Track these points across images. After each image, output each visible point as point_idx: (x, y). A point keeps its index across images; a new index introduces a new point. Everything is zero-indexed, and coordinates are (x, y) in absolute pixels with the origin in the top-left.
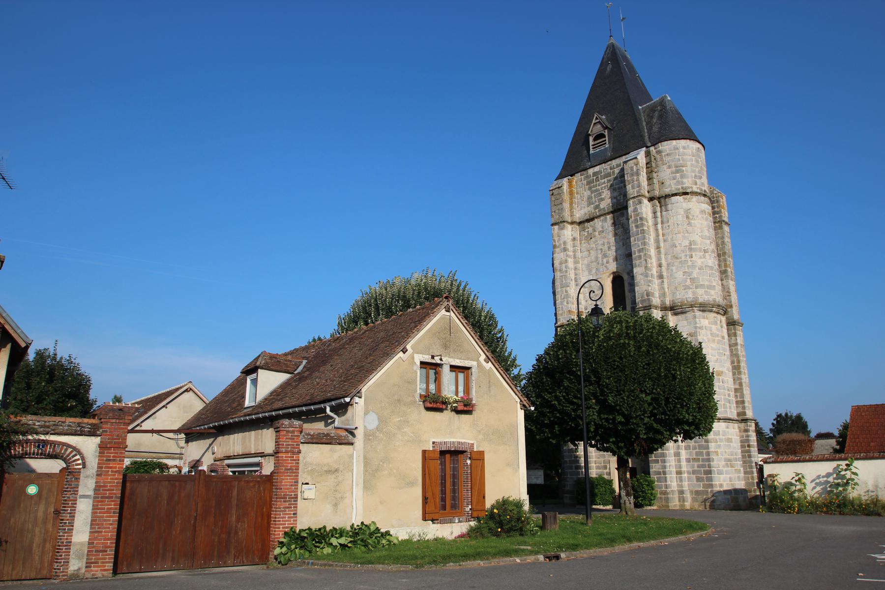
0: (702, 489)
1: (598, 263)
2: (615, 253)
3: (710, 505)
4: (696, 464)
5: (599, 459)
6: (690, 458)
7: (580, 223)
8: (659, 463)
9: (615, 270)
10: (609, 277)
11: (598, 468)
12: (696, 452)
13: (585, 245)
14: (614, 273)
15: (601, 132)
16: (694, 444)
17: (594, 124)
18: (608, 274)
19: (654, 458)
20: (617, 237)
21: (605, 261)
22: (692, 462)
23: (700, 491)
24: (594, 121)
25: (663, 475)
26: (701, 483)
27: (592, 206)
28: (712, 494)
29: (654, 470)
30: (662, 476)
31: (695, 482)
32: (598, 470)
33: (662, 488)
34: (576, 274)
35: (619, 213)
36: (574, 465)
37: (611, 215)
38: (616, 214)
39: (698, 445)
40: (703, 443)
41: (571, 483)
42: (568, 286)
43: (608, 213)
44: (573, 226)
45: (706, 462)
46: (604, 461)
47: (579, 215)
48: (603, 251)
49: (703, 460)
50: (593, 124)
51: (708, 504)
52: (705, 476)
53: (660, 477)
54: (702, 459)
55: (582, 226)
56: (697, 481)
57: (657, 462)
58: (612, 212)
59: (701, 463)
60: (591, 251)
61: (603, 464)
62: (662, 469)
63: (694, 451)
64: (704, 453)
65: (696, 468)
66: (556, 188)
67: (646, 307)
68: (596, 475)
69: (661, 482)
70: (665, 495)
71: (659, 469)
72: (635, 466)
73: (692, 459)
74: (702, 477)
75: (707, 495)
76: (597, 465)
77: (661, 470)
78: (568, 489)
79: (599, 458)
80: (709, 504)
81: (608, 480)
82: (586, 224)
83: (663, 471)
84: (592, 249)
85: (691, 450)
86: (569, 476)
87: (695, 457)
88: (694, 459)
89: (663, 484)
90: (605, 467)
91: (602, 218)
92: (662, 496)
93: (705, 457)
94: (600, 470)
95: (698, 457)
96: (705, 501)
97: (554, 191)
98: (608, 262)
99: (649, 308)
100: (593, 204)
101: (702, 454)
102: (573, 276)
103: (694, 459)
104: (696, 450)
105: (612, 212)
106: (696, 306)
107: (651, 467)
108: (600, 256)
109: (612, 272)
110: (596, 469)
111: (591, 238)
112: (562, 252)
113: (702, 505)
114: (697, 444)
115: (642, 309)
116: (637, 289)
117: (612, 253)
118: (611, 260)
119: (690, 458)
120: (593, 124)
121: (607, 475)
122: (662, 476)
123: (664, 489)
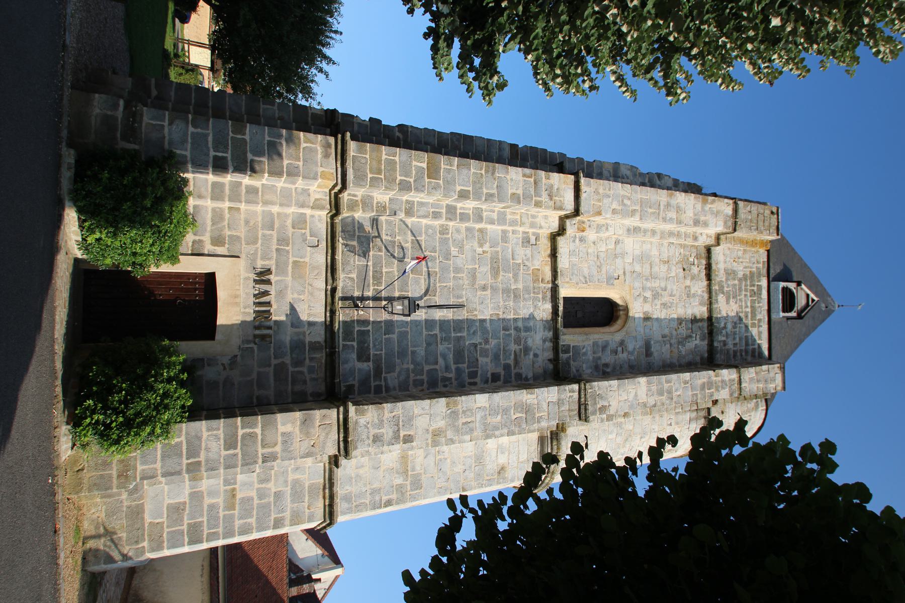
0: (148, 519)
1: (647, 279)
2: (655, 316)
3: (97, 550)
4: (220, 501)
5: (242, 222)
6: (235, 483)
7: (709, 250)
8: (226, 449)
9: (631, 314)
10: (622, 298)
11: (218, 216)
12: (253, 499)
13: (677, 254)
14: (626, 309)
15: (796, 305)
16: (273, 490)
17: (808, 296)
18: (628, 298)
19: (241, 432)
20: (675, 325)
21: (648, 294)
22: (226, 491)
23: (143, 519)
24: (812, 295)
25: (188, 464)
26: (165, 519)
27: (724, 279)
28: (130, 554)
29: (205, 434)
30: (185, 461)
31: (168, 501)
32: (210, 215)
33: (142, 464)
34: (645, 231)
35: (706, 331)
36: (229, 155)
37: (706, 315)
38: (705, 324)
39: (269, 503)
40: (273, 516)
41: (166, 130)
42: (641, 219)
43: (710, 310)
44: (713, 238)
45: (225, 528)
46: (238, 238)
47: (719, 253)
48: (663, 293)
49: (229, 520)
50: (809, 292)
51: (99, 544)
52: (185, 527)
53: (181, 455)
54: (233, 515)
55: (703, 252)
56: (169, 507)
57: (230, 444)
58: (710, 318)
59: (221, 514)
60: (666, 265)
61: (227, 233)
62: (207, 461)
63: (254, 494)
64: (249, 520)
65: (207, 501)
66: (778, 222)
67: (586, 409)
68: (195, 207)
69: (163, 457)
70: (119, 476)
71: (207, 449)
72: (219, 336)
73: (234, 489)
74: (182, 520)
75: (129, 541)
76: (227, 216)
77: (202, 457)
78: (146, 119)
79: (247, 222)
80: (102, 547)
81: (176, 243)
82: (704, 262)
83: (199, 463)
84: (669, 269)
85: (256, 486)
86: (191, 129)
87: (239, 496)
88: (234, 496)
89: (159, 465)
90: (218, 241)
91: (706, 296)
92: (114, 465)
93: (238, 523)
94: (209, 223)
95: (237, 506)
96: (109, 533)
97: (776, 216)
98: (645, 299)
99: (583, 416)
100: (727, 280)
101: (247, 513)
102: (648, 225)
103: (233, 494)
104: (256, 498)
105: (710, 318)
106: (549, 479)
107: (214, 423)
108: (656, 284)
109: (630, 306)
110: (214, 210)
111: (684, 270)
112: (695, 215)
113: (97, 527)
114: (272, 499)
115: (583, 400)
116: (614, 383)
117: (658, 313)
118: (647, 308)
119: (235, 483)
120: (809, 292)
121: (194, 242)
122: (185, 461)
123: (140, 468)
